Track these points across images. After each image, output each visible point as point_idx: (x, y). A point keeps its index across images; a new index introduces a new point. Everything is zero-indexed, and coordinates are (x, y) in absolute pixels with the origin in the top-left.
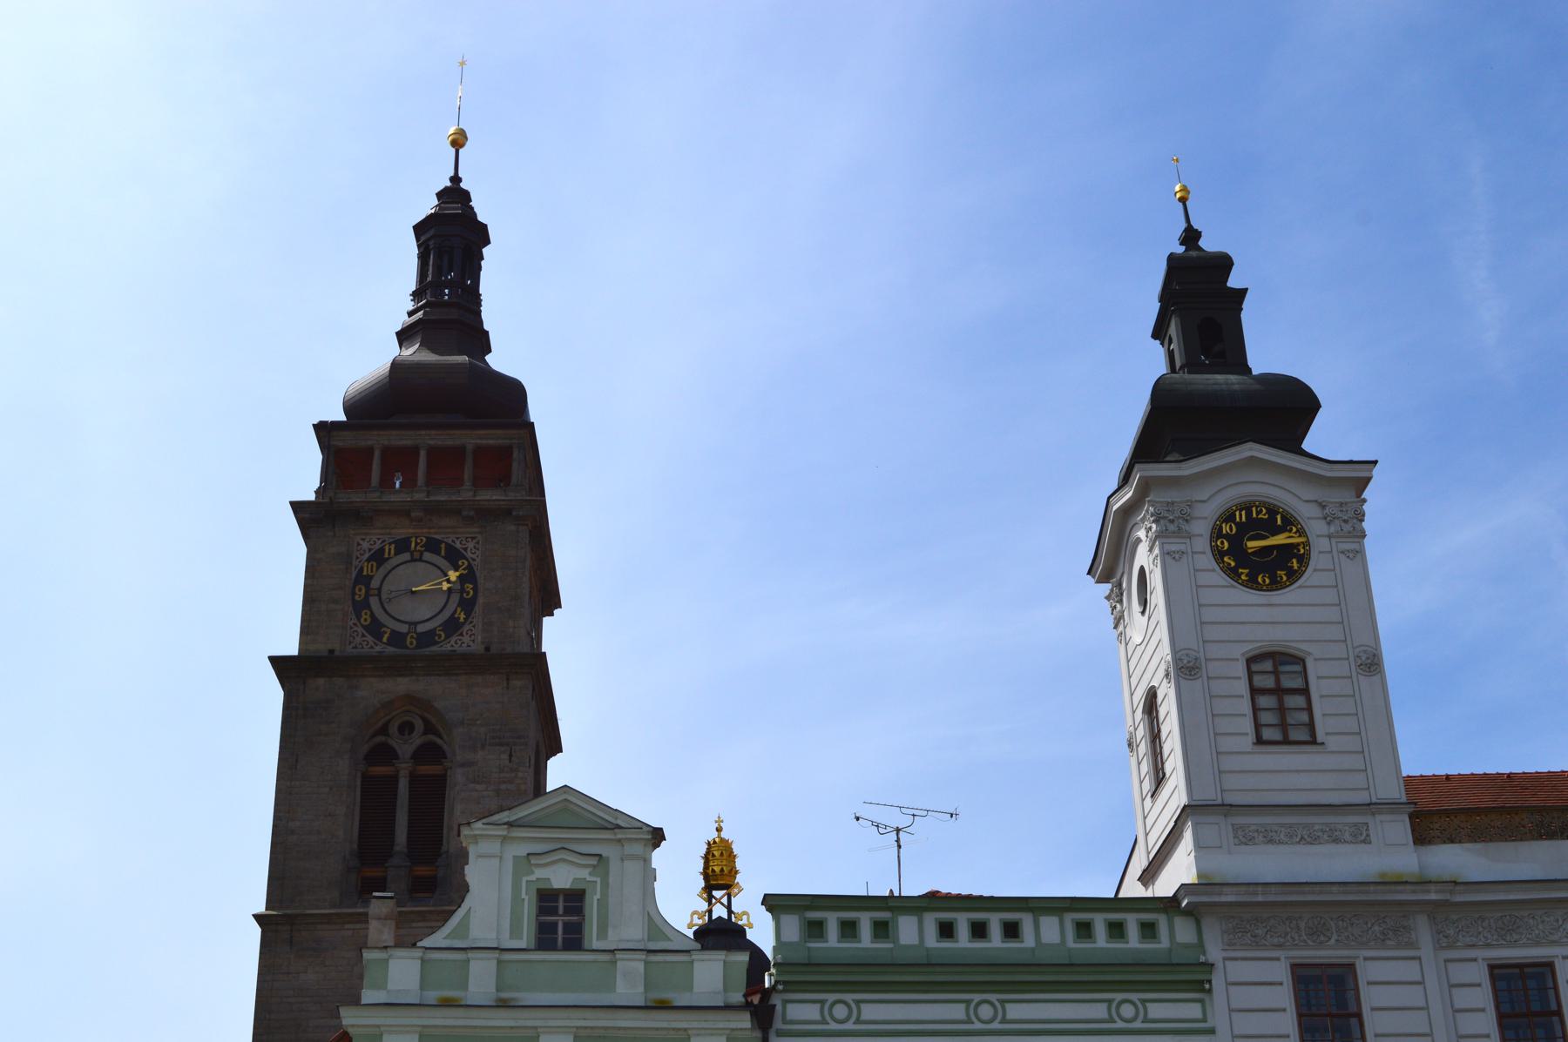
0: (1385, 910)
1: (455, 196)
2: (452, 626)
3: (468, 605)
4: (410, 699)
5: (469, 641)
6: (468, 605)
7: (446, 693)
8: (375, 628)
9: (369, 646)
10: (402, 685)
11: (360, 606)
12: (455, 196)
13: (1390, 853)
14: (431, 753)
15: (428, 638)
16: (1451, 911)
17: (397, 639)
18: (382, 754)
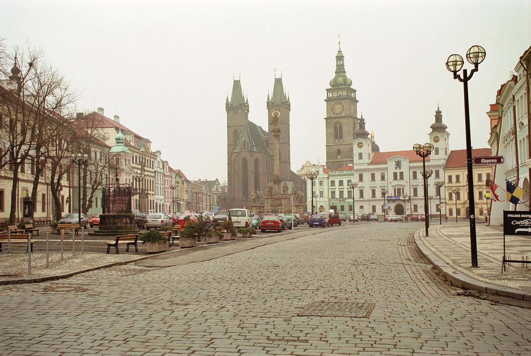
0: (365, 170)
1: (340, 52)
2: (342, 112)
3: (343, 110)
4: (338, 121)
5: (343, 114)
6: (343, 110)
7: (341, 120)
8: (334, 113)
9: (334, 116)
10: (336, 120)
11: (332, 111)
12: (340, 52)
13: (366, 167)
14: (341, 127)
15: (339, 114)
16: (369, 170)
17: (336, 114)
18: (336, 127)
